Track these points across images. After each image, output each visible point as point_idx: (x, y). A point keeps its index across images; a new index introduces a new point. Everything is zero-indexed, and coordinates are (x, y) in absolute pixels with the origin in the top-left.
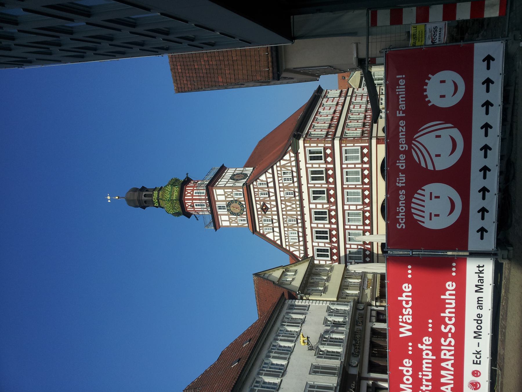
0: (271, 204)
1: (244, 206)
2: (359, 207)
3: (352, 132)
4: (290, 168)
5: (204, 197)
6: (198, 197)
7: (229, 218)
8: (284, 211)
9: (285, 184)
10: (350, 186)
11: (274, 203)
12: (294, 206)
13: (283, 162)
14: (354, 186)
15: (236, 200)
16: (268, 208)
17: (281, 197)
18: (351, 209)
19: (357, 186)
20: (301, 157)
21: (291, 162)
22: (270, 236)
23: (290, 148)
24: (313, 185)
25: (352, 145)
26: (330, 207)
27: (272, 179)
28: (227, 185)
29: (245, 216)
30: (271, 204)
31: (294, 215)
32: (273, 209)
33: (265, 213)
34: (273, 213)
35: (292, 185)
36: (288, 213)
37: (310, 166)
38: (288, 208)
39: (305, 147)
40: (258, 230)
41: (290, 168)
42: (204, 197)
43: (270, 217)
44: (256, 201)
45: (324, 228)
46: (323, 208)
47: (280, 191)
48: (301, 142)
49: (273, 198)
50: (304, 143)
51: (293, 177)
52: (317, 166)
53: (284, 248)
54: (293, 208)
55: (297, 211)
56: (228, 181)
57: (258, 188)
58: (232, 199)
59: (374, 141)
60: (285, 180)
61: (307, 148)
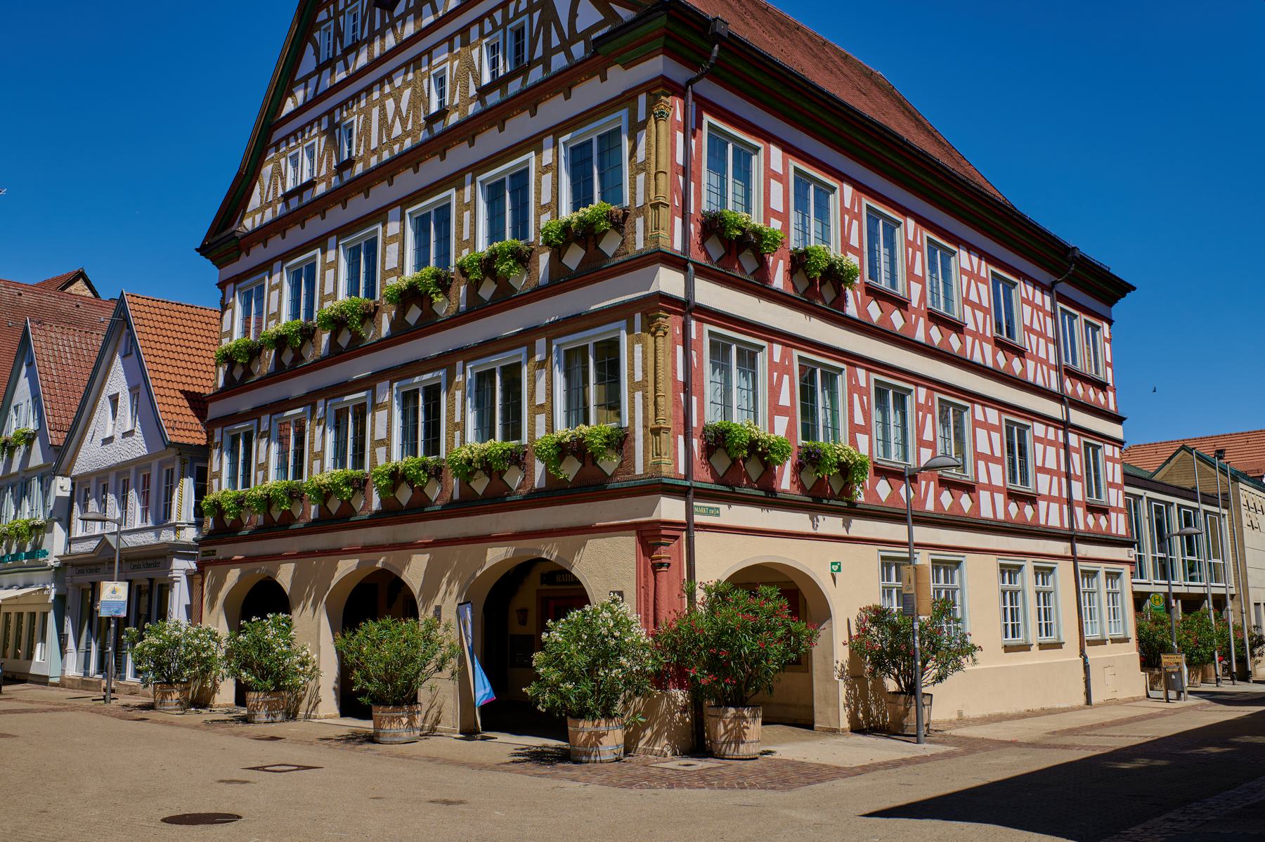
0: (403, 18)
4: (539, 52)
12: (397, 130)
14: (458, 419)
16: (392, 9)
20: (589, 93)
22: (308, 63)
24: (467, 199)
25: (639, 376)
36: (375, 112)
38: (390, 104)
45: (322, 300)
48: (656, 66)
52: (546, 198)
53: (269, 136)
60: (494, 49)
61: (623, 114)
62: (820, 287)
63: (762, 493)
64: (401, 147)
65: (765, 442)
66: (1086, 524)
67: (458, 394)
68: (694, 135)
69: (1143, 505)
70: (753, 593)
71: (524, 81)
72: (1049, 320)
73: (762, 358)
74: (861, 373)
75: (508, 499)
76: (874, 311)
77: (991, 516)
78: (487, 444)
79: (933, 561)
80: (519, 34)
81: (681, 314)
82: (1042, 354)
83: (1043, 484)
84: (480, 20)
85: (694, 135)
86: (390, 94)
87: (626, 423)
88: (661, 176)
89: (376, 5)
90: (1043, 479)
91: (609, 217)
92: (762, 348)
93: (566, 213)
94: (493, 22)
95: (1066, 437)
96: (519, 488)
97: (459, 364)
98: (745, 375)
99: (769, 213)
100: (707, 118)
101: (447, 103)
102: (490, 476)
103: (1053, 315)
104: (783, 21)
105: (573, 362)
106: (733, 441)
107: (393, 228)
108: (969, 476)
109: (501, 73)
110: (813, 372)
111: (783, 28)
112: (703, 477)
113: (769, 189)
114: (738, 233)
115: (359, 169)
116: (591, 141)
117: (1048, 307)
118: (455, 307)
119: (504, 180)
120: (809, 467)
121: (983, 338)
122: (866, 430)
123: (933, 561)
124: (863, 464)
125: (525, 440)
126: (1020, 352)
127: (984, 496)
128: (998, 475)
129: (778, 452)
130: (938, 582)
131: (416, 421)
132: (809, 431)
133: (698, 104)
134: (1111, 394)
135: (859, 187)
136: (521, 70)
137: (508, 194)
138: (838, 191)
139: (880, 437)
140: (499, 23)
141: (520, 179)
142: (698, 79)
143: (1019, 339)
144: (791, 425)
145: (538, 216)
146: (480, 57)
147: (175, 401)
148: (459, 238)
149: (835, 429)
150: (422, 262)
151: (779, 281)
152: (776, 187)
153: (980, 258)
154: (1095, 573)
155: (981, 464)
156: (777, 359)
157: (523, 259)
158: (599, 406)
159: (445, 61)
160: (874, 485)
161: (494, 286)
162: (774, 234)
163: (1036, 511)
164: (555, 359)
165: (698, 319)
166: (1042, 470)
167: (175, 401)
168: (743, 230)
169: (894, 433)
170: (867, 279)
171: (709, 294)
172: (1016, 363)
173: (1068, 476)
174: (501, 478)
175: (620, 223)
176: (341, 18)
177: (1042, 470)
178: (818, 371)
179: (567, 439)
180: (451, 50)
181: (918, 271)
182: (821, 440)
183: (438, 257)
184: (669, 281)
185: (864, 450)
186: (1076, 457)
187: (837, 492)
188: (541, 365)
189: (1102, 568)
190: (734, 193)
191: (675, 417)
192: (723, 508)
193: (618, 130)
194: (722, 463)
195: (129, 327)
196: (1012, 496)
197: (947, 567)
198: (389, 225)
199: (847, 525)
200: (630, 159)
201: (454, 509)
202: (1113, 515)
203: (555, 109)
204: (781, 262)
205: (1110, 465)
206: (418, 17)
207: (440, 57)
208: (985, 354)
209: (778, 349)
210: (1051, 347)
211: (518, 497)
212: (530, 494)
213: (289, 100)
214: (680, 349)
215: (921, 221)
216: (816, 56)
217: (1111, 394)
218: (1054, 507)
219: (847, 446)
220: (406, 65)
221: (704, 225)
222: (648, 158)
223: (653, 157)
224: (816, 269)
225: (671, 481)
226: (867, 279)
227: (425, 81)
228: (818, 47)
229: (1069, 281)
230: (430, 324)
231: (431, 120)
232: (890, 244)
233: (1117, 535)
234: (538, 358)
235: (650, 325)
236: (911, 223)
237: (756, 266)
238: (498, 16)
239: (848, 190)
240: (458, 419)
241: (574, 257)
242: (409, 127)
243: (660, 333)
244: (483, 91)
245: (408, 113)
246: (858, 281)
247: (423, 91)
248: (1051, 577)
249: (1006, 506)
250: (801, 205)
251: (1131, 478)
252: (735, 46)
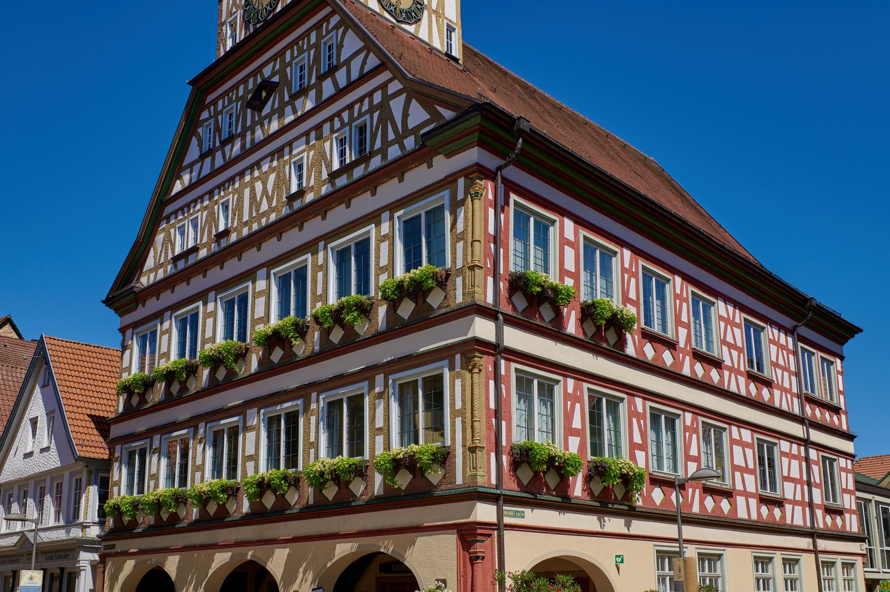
4: (378, 145)
14: (312, 439)
16: (260, 110)
20: (419, 177)
24: (320, 261)
25: (459, 405)
36: (247, 192)
38: (259, 186)
40: (210, 98)
44: (282, 53)
52: (384, 262)
57: (317, 46)
60: (342, 142)
61: (446, 193)
62: (605, 332)
63: (559, 499)
64: (267, 220)
65: (560, 457)
66: (825, 523)
67: (313, 419)
68: (503, 210)
69: (872, 507)
70: (552, 580)
71: (366, 168)
72: (791, 357)
73: (558, 390)
74: (639, 401)
75: (353, 504)
76: (649, 351)
77: (746, 517)
78: (336, 460)
79: (699, 554)
80: (362, 130)
81: (493, 355)
82: (786, 385)
83: (789, 491)
84: (331, 119)
85: (503, 210)
86: (259, 178)
87: (448, 443)
88: (476, 244)
89: (247, 107)
90: (789, 487)
91: (435, 276)
92: (558, 382)
93: (400, 273)
94: (342, 120)
95: (807, 452)
96: (361, 495)
97: (314, 395)
98: (545, 404)
99: (563, 273)
100: (513, 197)
101: (304, 185)
102: (339, 485)
103: (795, 353)
104: (574, 118)
105: (406, 393)
106: (535, 457)
107: (261, 285)
108: (727, 484)
109: (348, 161)
110: (600, 401)
111: (574, 124)
112: (511, 486)
113: (563, 253)
114: (539, 289)
116: (420, 216)
117: (791, 347)
118: (310, 349)
119: (350, 247)
120: (597, 478)
121: (738, 372)
122: (643, 447)
123: (699, 554)
124: (641, 475)
125: (367, 456)
126: (768, 384)
127: (740, 501)
128: (751, 483)
129: (571, 465)
130: (703, 571)
131: (279, 440)
132: (597, 449)
133: (505, 186)
134: (843, 417)
135: (637, 252)
136: (363, 158)
137: (353, 258)
138: (619, 255)
139: (655, 453)
140: (346, 121)
141: (363, 247)
142: (505, 166)
143: (768, 372)
144: (582, 444)
145: (377, 276)
146: (331, 148)
147: (84, 423)
148: (314, 293)
149: (618, 447)
150: (284, 312)
151: (572, 327)
152: (569, 252)
153: (735, 308)
154: (833, 564)
155: (738, 475)
156: (570, 390)
157: (365, 310)
158: (426, 429)
159: (303, 151)
160: (650, 492)
161: (342, 330)
162: (567, 290)
163: (783, 513)
164: (391, 391)
165: (506, 359)
166: (788, 479)
167: (84, 423)
168: (542, 287)
169: (666, 450)
170: (643, 325)
171: (516, 339)
172: (765, 392)
173: (809, 484)
174: (347, 487)
175: (443, 281)
176: (220, 117)
177: (788, 479)
178: (604, 400)
179: (401, 456)
180: (307, 142)
181: (684, 318)
182: (607, 456)
183: (297, 309)
184: (483, 329)
185: (641, 463)
186: (815, 468)
187: (619, 498)
188: (380, 395)
189: (839, 560)
190: (535, 257)
191: (488, 438)
192: (527, 511)
193: (441, 208)
194: (526, 475)
195: (47, 363)
196: (764, 500)
197: (710, 559)
198: (257, 283)
199: (628, 525)
200: (451, 230)
201: (308, 512)
202: (847, 516)
203: (391, 190)
204: (573, 312)
205: (843, 474)
206: (281, 115)
207: (299, 147)
208: (739, 385)
209: (571, 382)
210: (794, 378)
211: (361, 503)
212: (371, 500)
213: (178, 182)
214: (492, 383)
215: (688, 279)
216: (601, 146)
217: (843, 417)
218: (798, 509)
219: (628, 461)
220: (272, 155)
221: (511, 283)
222: (465, 230)
223: (470, 229)
224: (602, 318)
225: (485, 490)
226: (643, 325)
227: (287, 167)
228: (602, 139)
229: (807, 325)
230: (290, 363)
231: (292, 198)
232: (662, 297)
233: (851, 532)
234: (377, 390)
235: (469, 365)
236: (678, 280)
237: (553, 315)
238: (345, 115)
239: (627, 253)
240: (312, 439)
241: (406, 309)
243: (476, 370)
244: (333, 176)
246: (635, 327)
247: (285, 175)
248: (796, 567)
249: (759, 509)
250: (589, 265)
251: (861, 485)
252: (535, 139)
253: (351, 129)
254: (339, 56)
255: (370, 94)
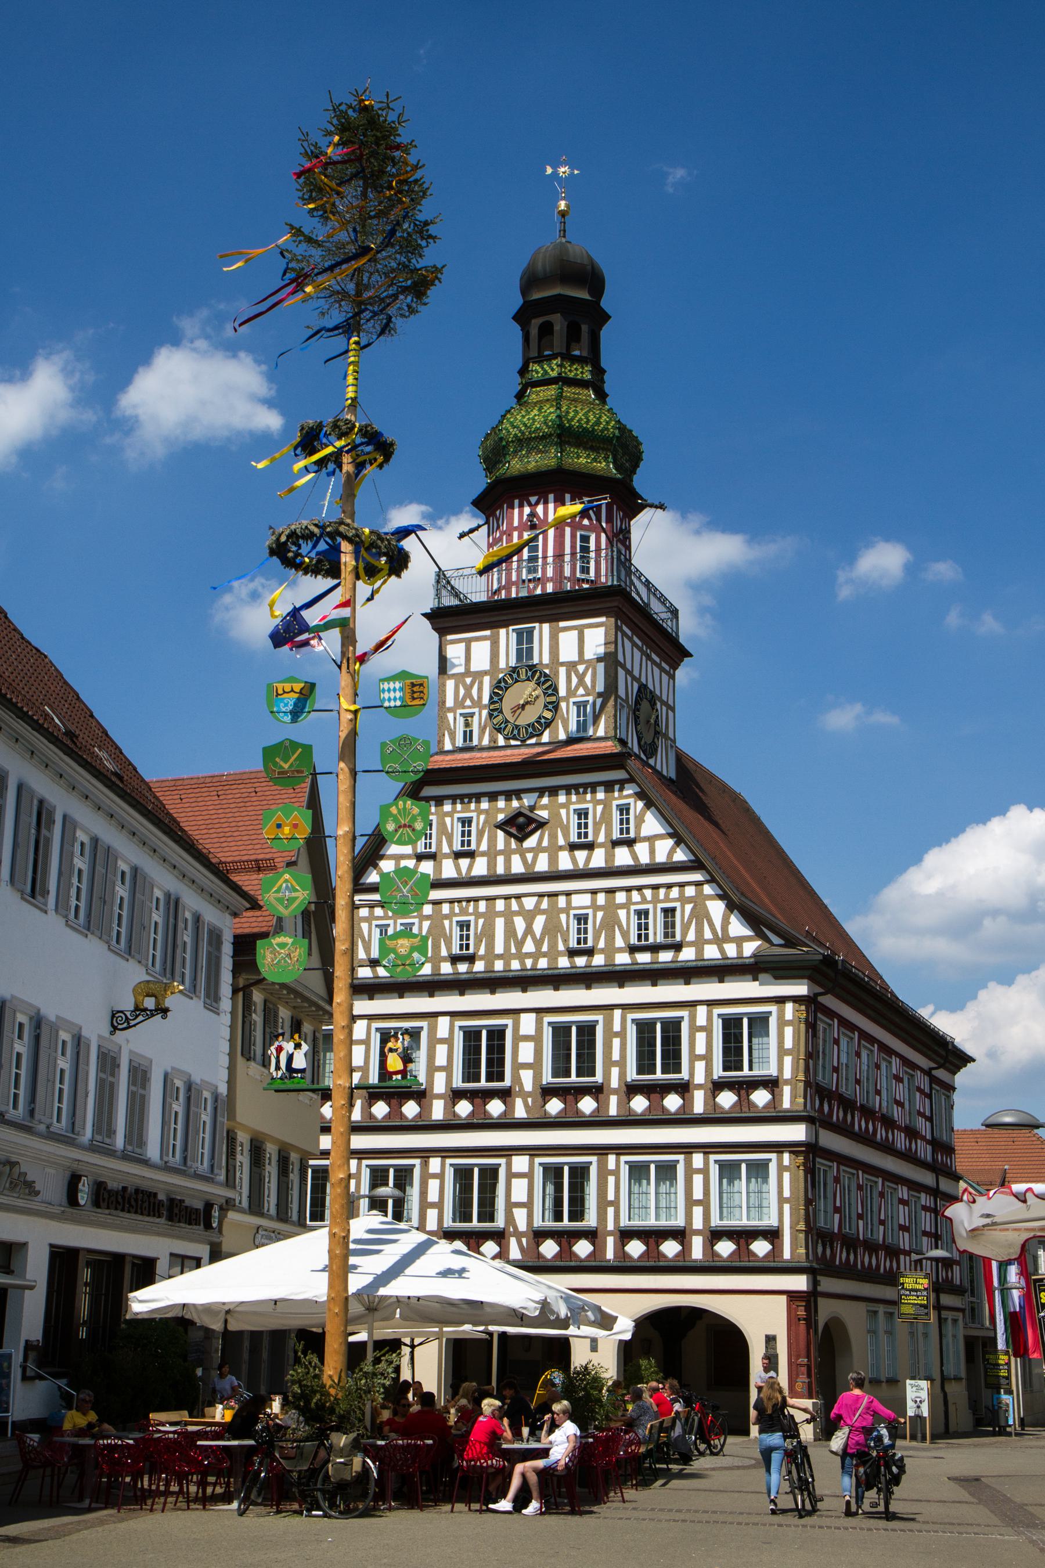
1: (533, 741)
2: (520, 1216)
3: (830, 1195)
4: (691, 936)
5: (567, 572)
6: (568, 550)
7: (479, 675)
8: (508, 906)
9: (622, 913)
10: (611, 1179)
11: (542, 865)
12: (529, 947)
13: (717, 908)
14: (611, 1197)
15: (555, 707)
16: (521, 840)
17: (568, 894)
18: (515, 1181)
19: (611, 1211)
21: (720, 940)
23: (776, 940)
24: (617, 1027)
25: (787, 1193)
26: (524, 1095)
27: (644, 859)
28: (621, 673)
29: (486, 742)
30: (537, 850)
31: (490, 946)
32: (516, 859)
33: (500, 826)
34: (500, 860)
35: (619, 942)
36: (500, 923)
37: (701, 1019)
38: (520, 924)
39: (781, 1000)
41: (691, 936)
42: (567, 572)
43: (484, 847)
46: (518, 1066)
47: (594, 892)
49: (565, 863)
50: (795, 999)
51: (655, 949)
52: (701, 1049)
54: (520, 944)
55: (506, 957)
56: (634, 678)
58: (562, 692)
59: (799, 1283)
60: (642, 914)
115: (479, 966)
140: (649, 898)
242: (545, 948)
245: (543, 935)
253: (655, 908)
254: (638, 827)
255: (682, 885)
